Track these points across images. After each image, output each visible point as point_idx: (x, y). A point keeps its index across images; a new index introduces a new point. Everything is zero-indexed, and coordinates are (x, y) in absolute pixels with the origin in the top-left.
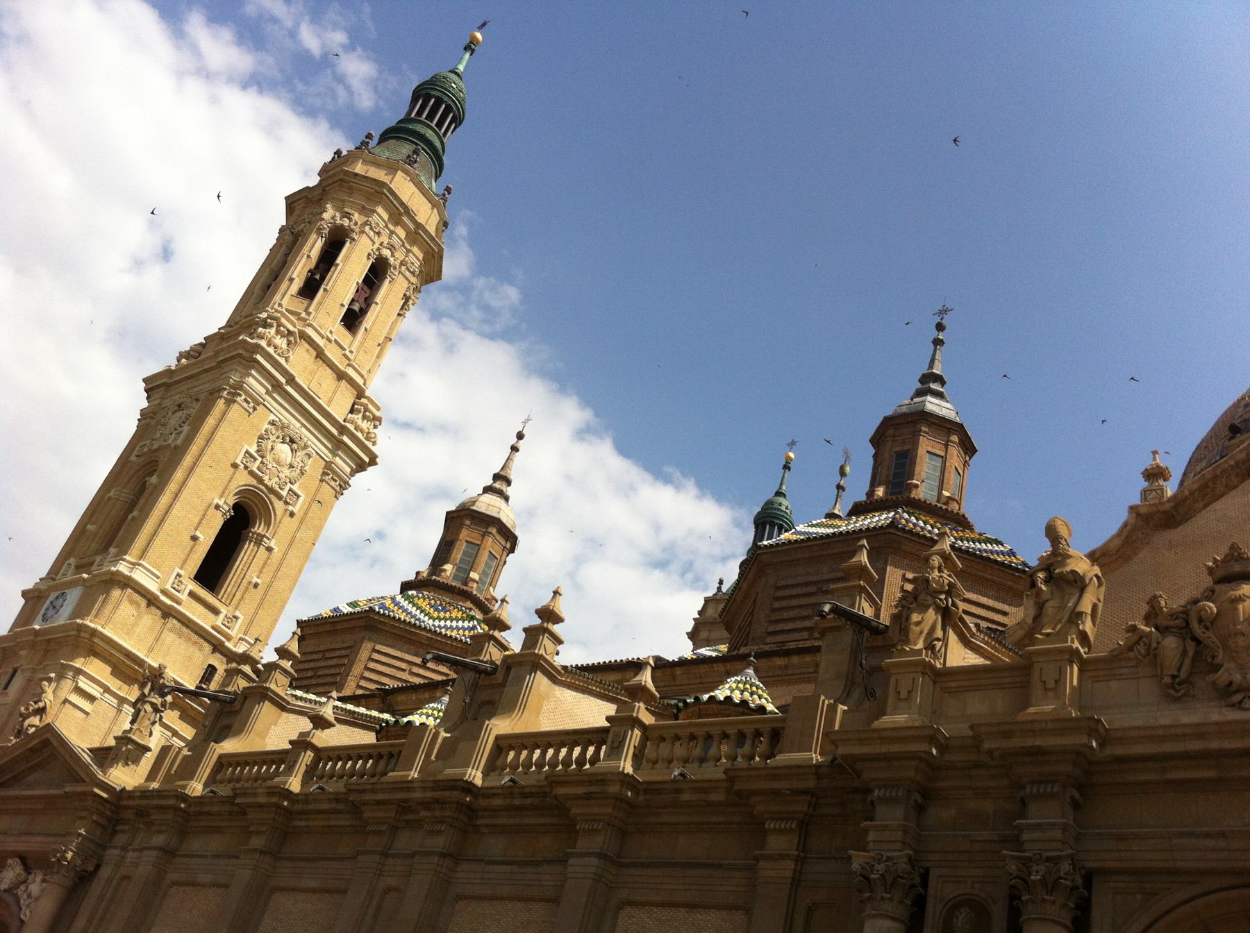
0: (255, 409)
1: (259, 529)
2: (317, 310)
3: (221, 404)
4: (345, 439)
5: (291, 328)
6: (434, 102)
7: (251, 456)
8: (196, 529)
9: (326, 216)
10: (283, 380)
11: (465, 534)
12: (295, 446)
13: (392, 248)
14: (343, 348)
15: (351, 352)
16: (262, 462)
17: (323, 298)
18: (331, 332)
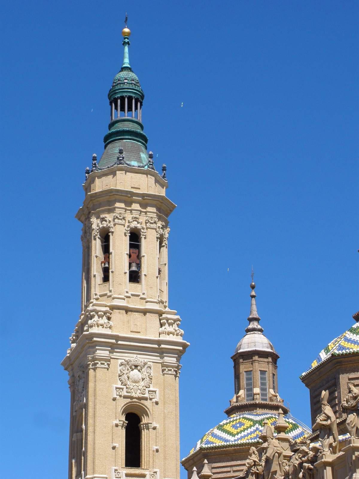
0: (109, 365)
1: (145, 420)
2: (113, 287)
3: (91, 372)
4: (163, 346)
5: (104, 309)
6: (120, 102)
7: (120, 388)
8: (112, 443)
9: (94, 226)
10: (114, 341)
11: (243, 368)
12: (139, 368)
13: (135, 219)
14: (138, 296)
15: (144, 294)
16: (127, 388)
17: (113, 277)
18: (127, 292)
